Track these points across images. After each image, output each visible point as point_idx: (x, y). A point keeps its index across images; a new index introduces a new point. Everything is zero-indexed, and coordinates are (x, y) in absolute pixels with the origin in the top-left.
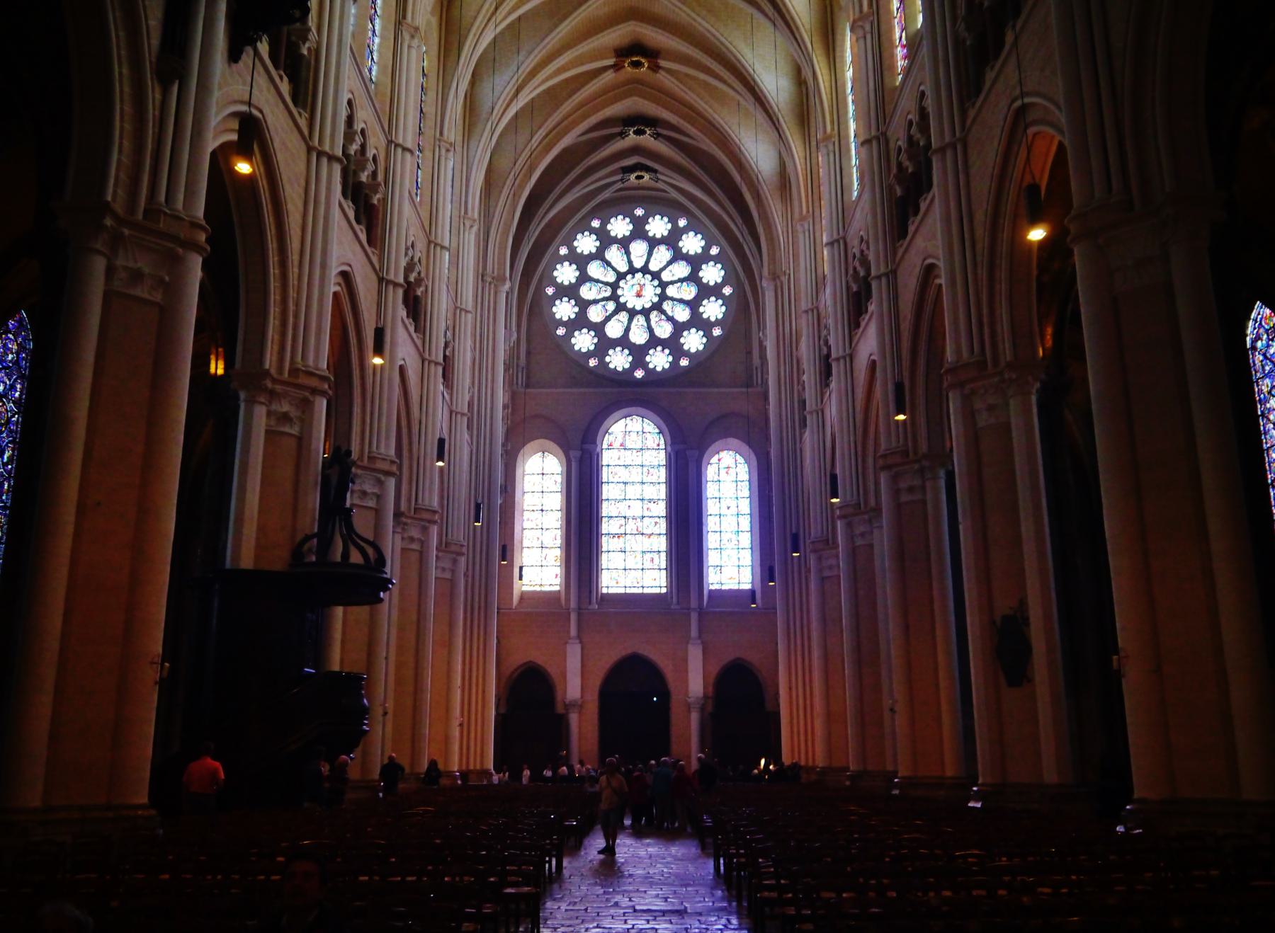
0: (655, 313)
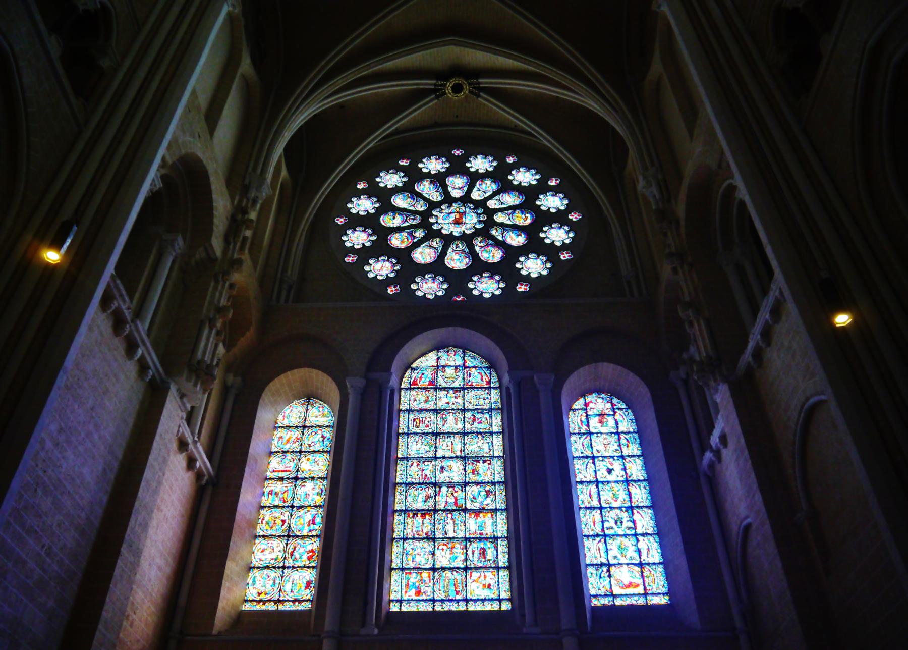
0: (479, 239)
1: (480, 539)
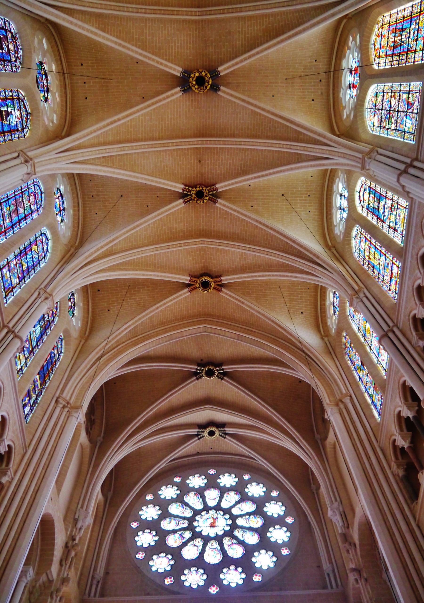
0: (227, 538)
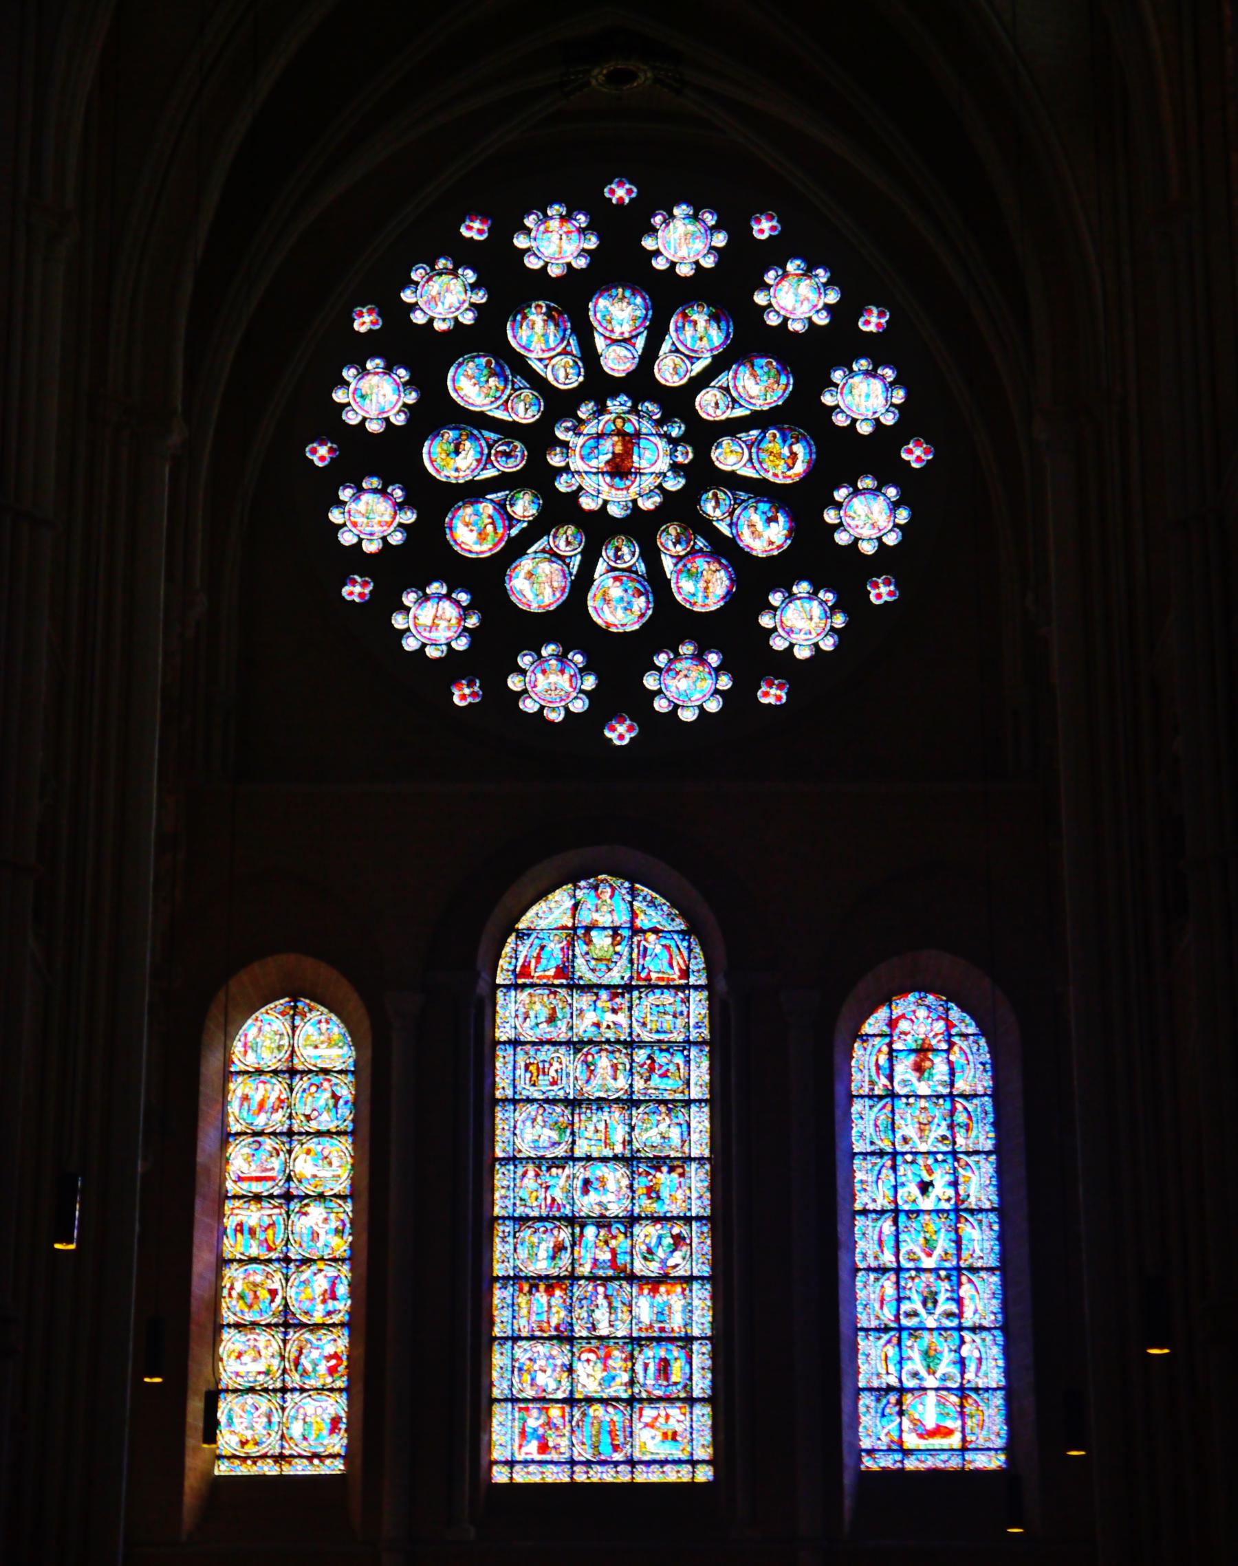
0: (673, 530)
1: (659, 1340)
